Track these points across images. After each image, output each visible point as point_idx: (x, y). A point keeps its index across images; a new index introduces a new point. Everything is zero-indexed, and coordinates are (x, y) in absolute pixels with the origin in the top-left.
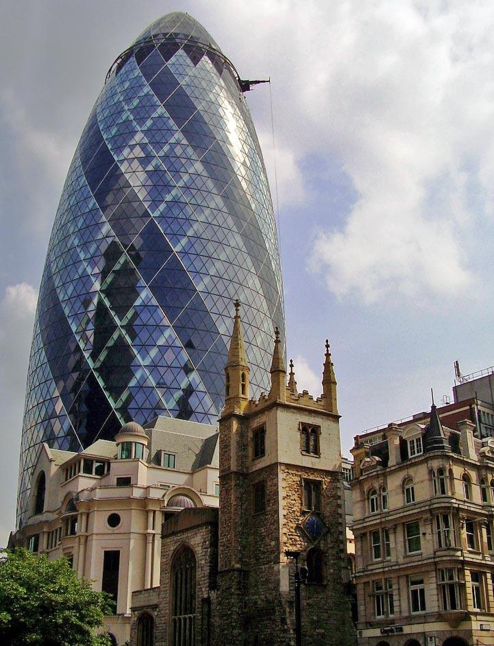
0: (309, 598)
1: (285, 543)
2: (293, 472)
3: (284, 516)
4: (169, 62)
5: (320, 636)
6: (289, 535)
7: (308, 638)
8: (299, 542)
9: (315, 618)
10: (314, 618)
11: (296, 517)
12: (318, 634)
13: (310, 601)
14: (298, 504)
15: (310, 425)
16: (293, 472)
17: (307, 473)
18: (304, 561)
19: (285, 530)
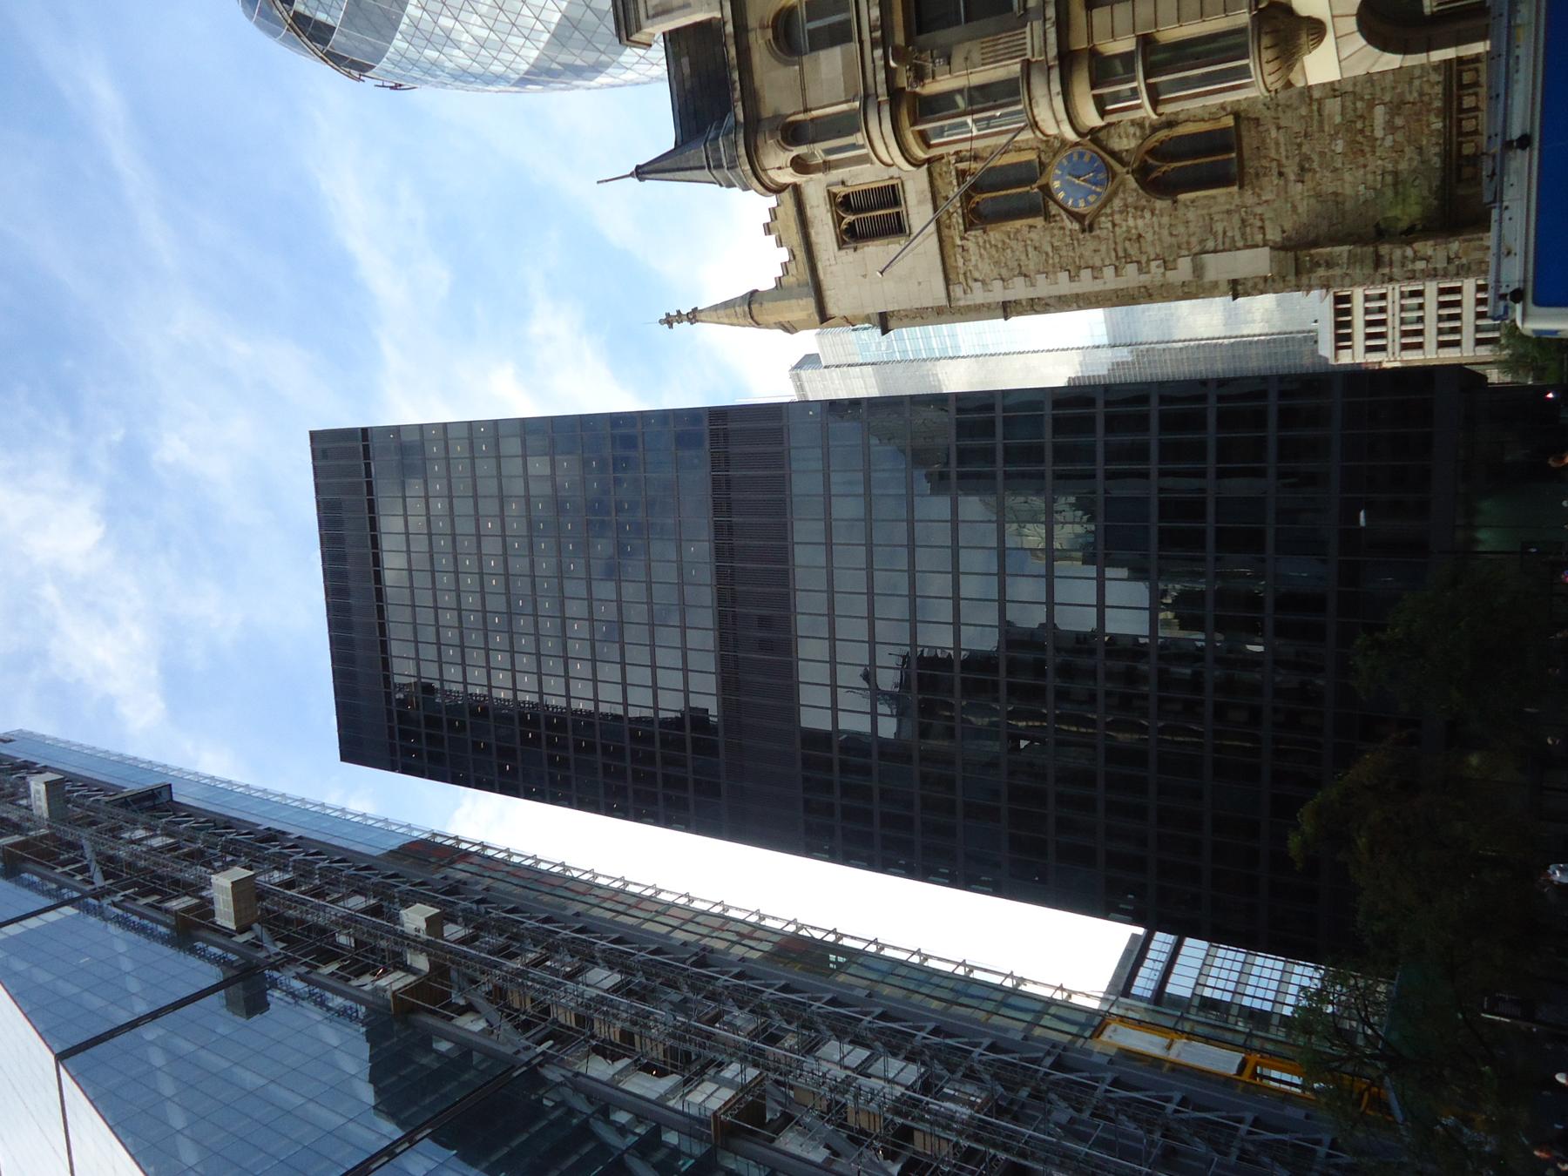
0: (1281, 174)
1: (1140, 271)
2: (960, 262)
3: (1071, 279)
4: (330, 22)
5: (1399, 121)
6: (1117, 257)
7: (1403, 166)
8: (1131, 222)
9: (1340, 146)
10: (1339, 149)
11: (1068, 240)
12: (1391, 128)
13: (1291, 171)
14: (1033, 235)
15: (838, 220)
16: (960, 262)
17: (950, 215)
18: (1175, 202)
19: (1109, 272)
